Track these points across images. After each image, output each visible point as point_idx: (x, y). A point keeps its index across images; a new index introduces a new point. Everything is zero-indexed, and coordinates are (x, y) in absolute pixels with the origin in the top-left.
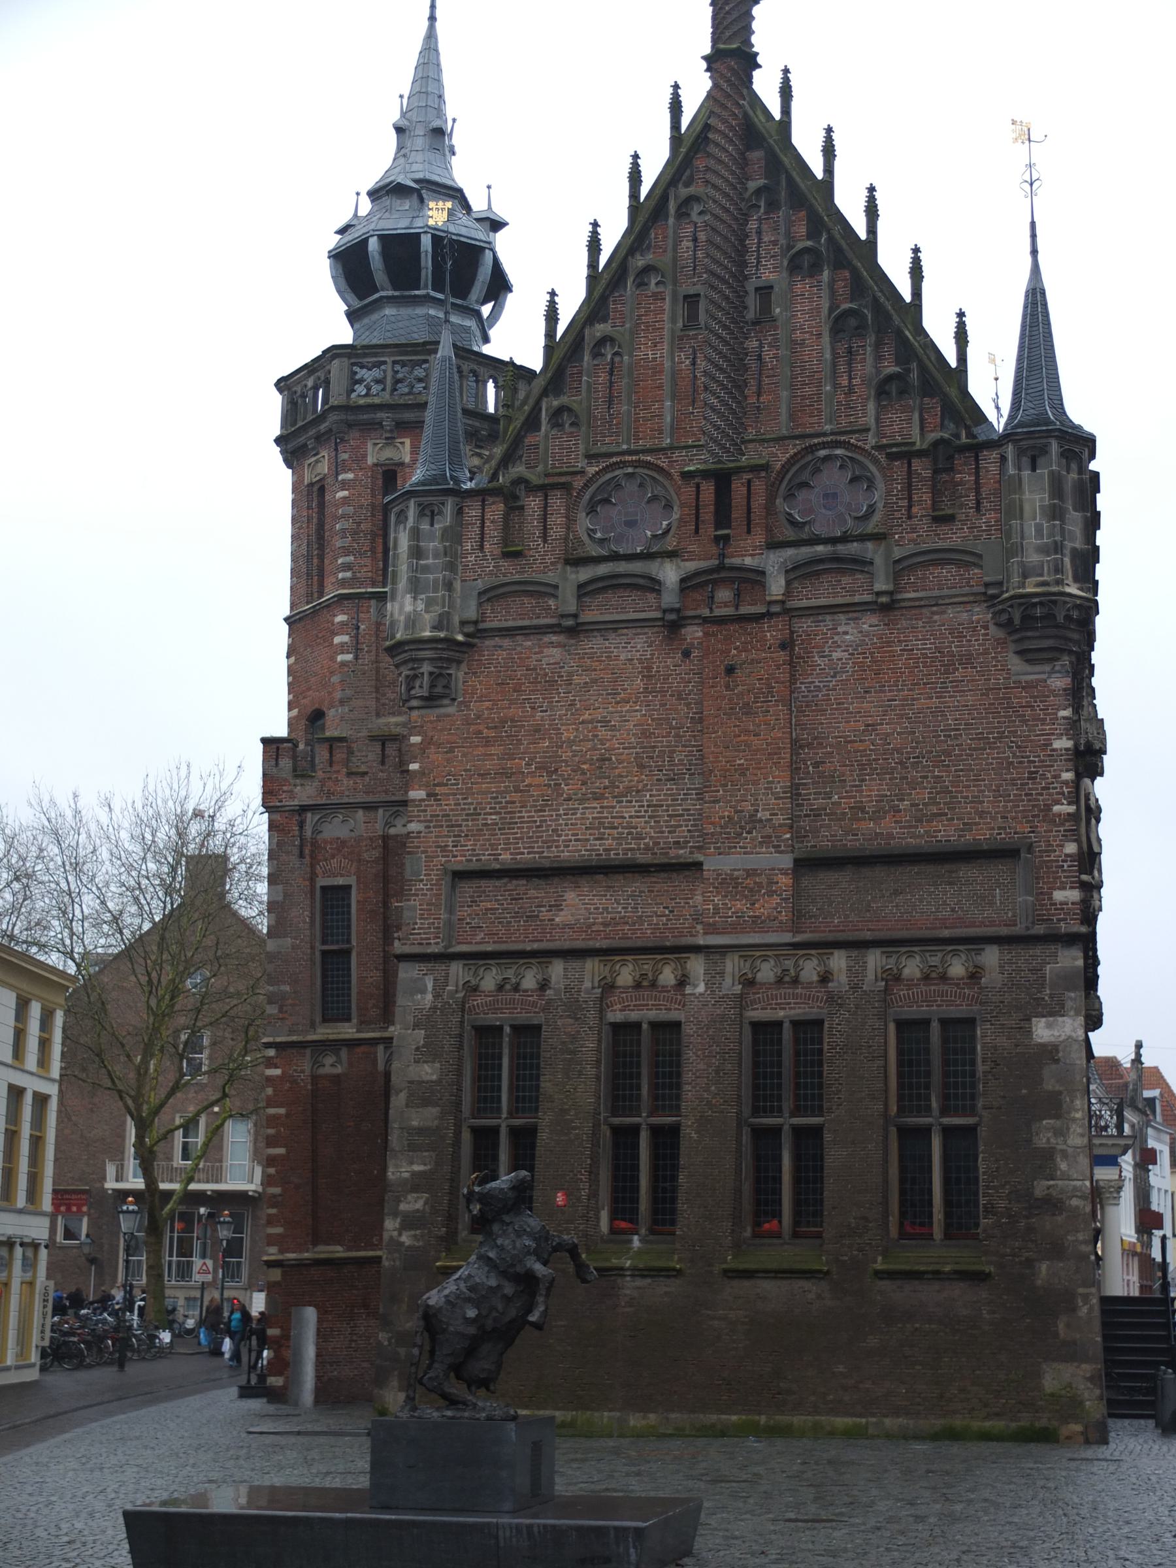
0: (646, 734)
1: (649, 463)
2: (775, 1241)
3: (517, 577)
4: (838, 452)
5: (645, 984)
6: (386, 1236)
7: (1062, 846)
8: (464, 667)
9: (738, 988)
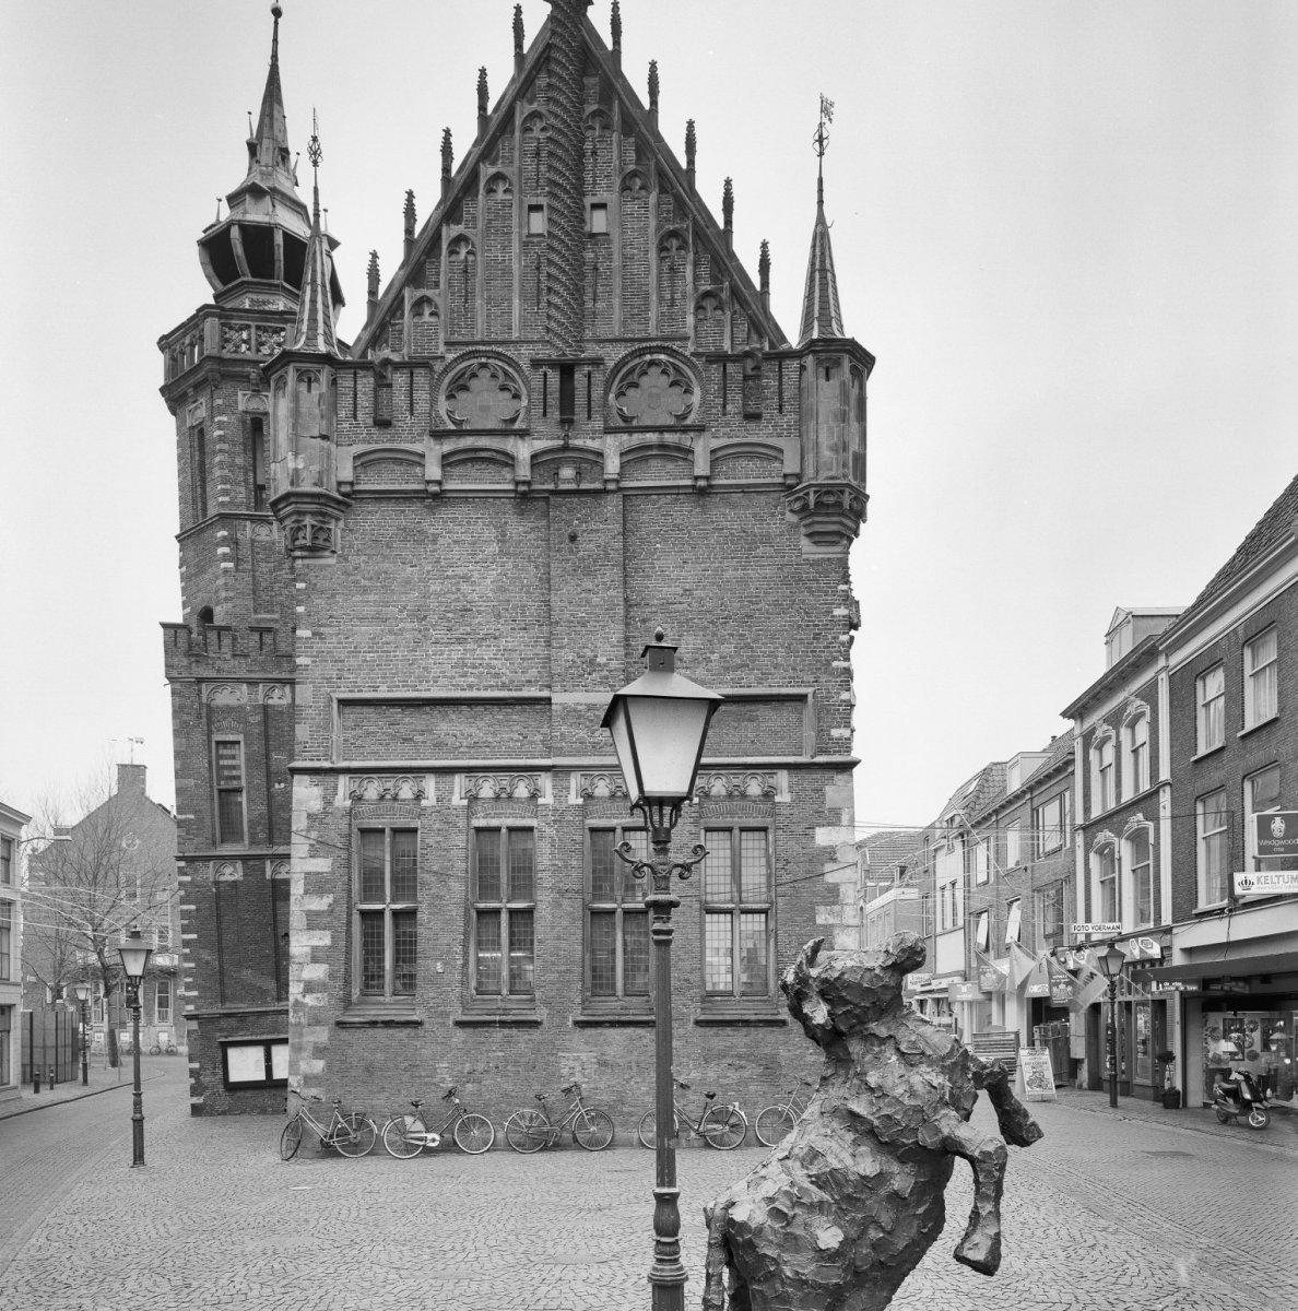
0: (502, 590)
1: (498, 353)
2: (612, 998)
3: (388, 446)
4: (662, 357)
5: (503, 798)
6: (291, 998)
7: (839, 693)
8: (341, 524)
9: (580, 801)
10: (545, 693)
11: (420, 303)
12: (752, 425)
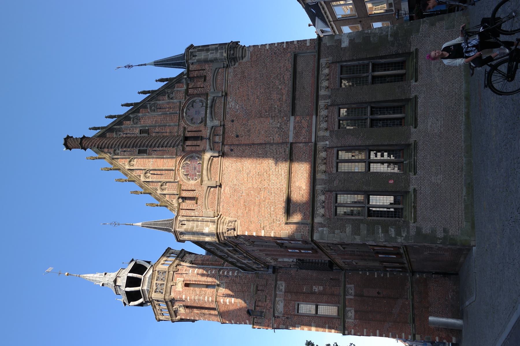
4: (185, 110)
10: (289, 145)
12: (208, 78)
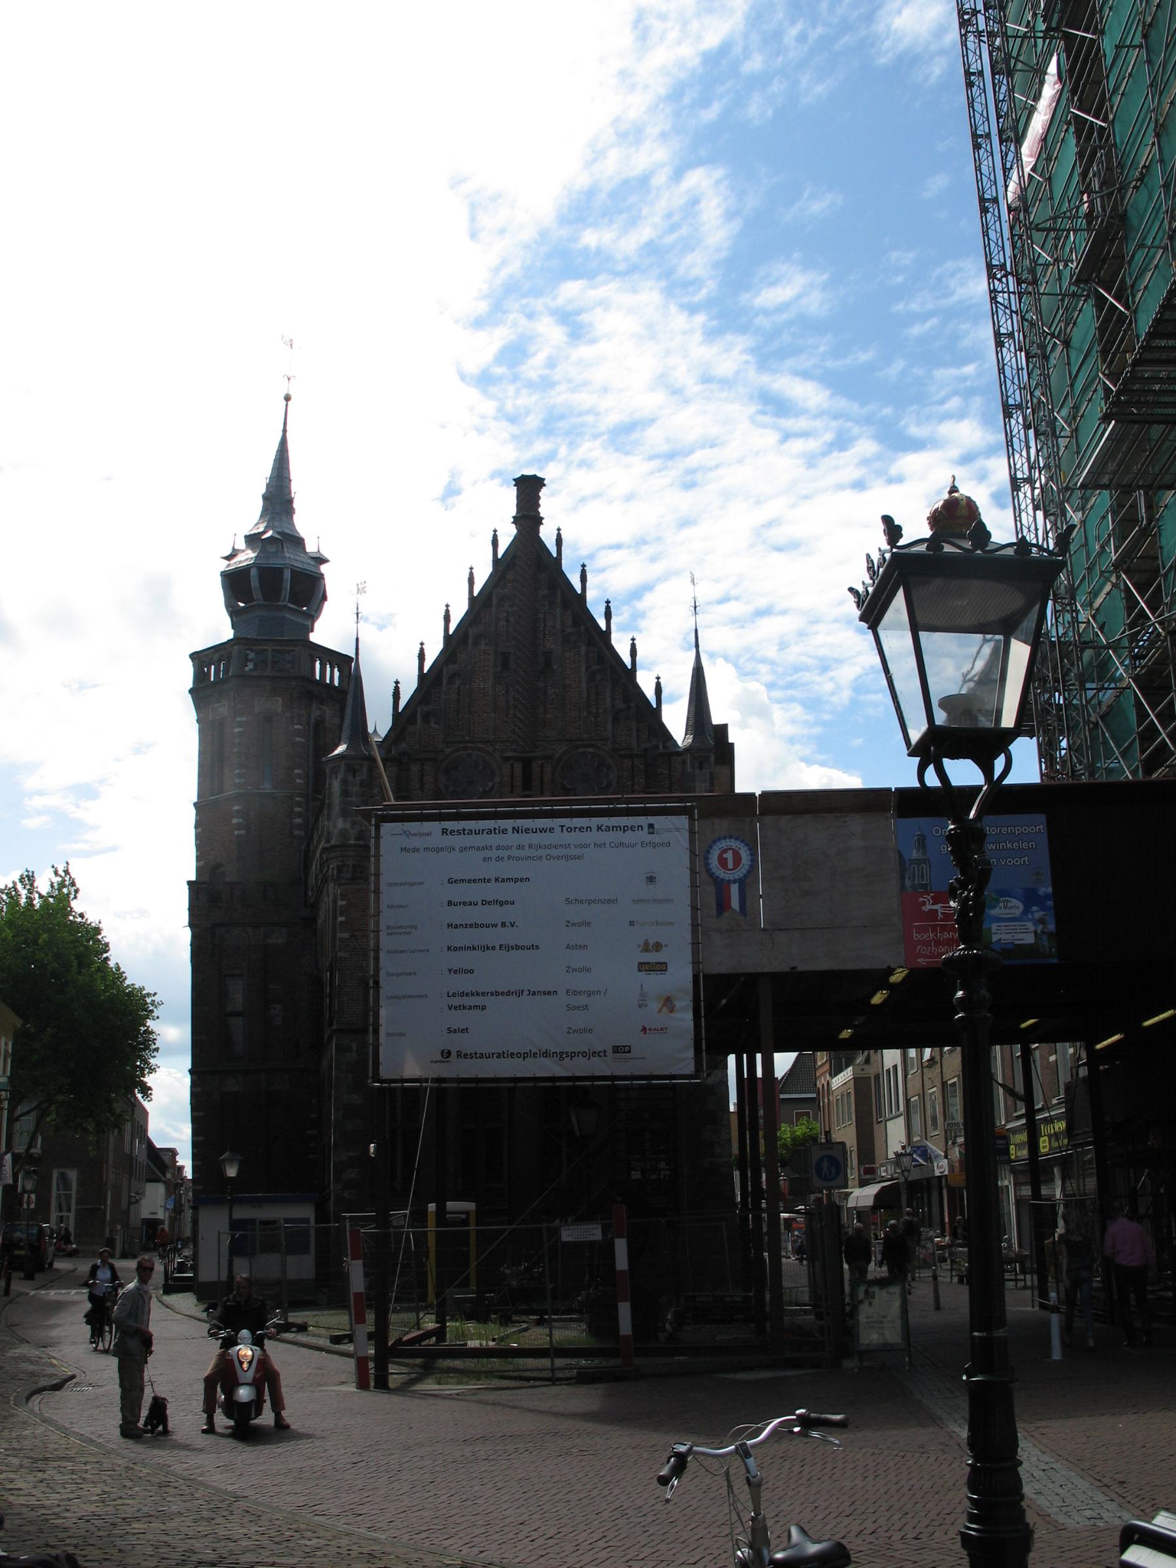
4: (591, 750)
11: (426, 717)
